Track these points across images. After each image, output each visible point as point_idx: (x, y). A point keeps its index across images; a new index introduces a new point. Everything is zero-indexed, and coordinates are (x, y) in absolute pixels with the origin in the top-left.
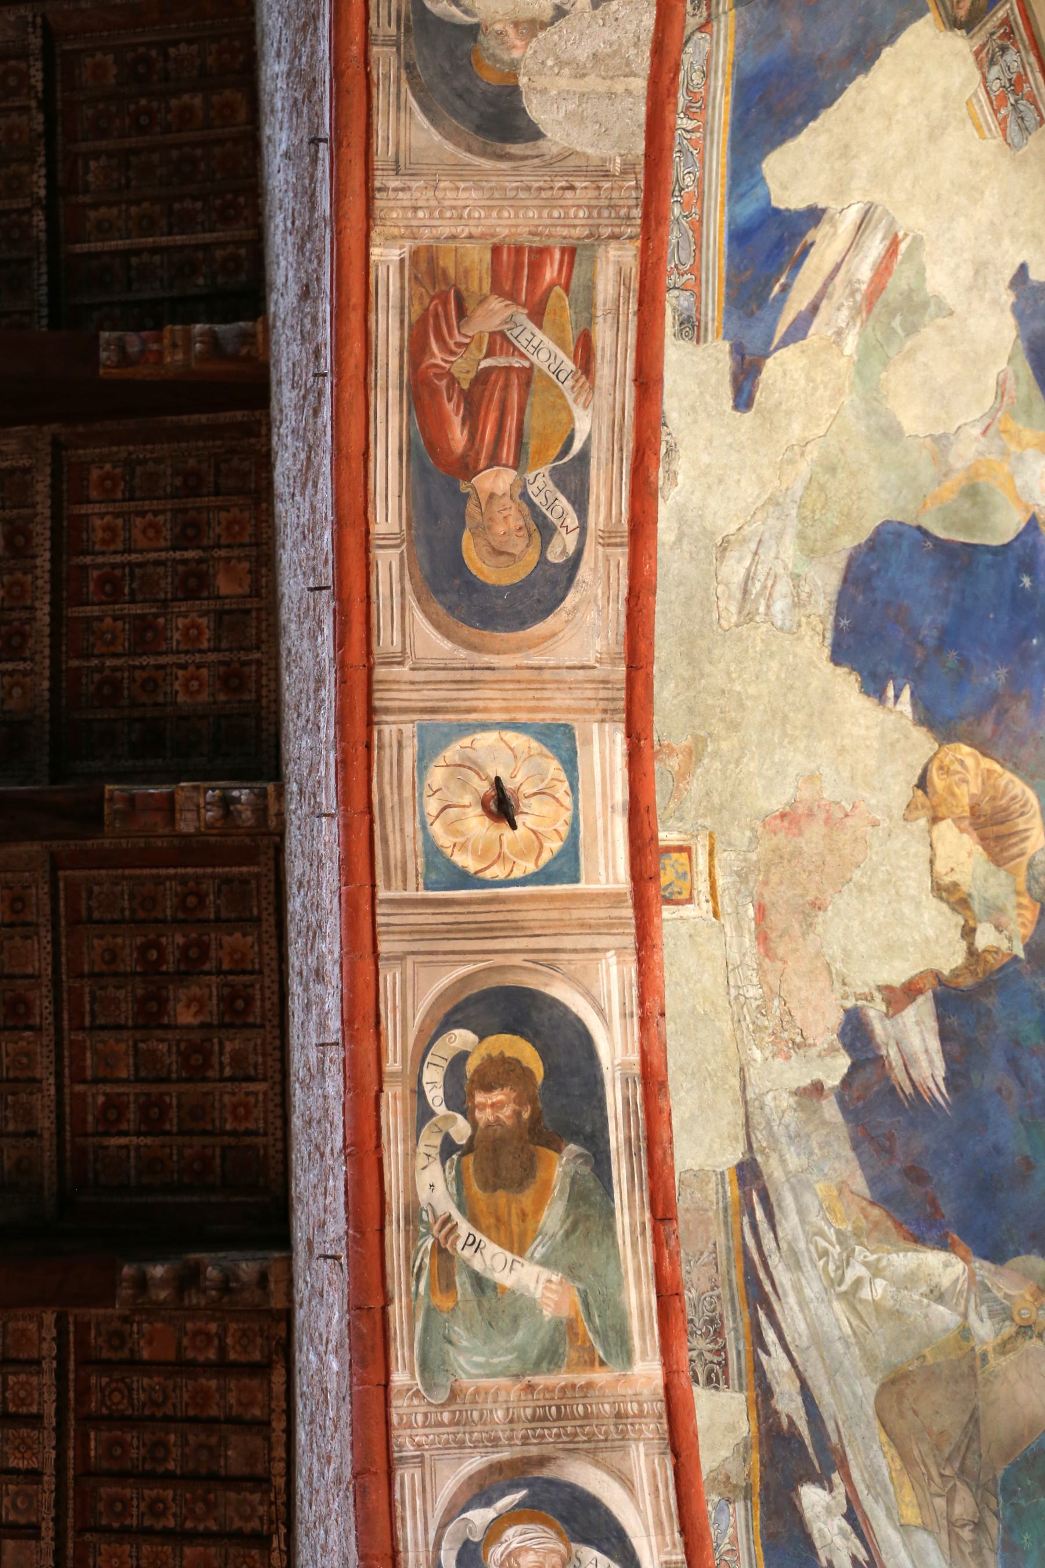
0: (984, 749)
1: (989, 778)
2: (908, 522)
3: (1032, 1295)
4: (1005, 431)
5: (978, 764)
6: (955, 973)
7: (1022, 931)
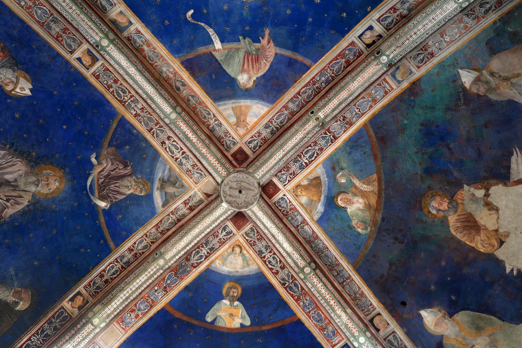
0: (473, 249)
1: (472, 240)
2: (508, 324)
3: (500, 89)
4: (464, 345)
5: (476, 245)
6: (497, 184)
7: (463, 192)
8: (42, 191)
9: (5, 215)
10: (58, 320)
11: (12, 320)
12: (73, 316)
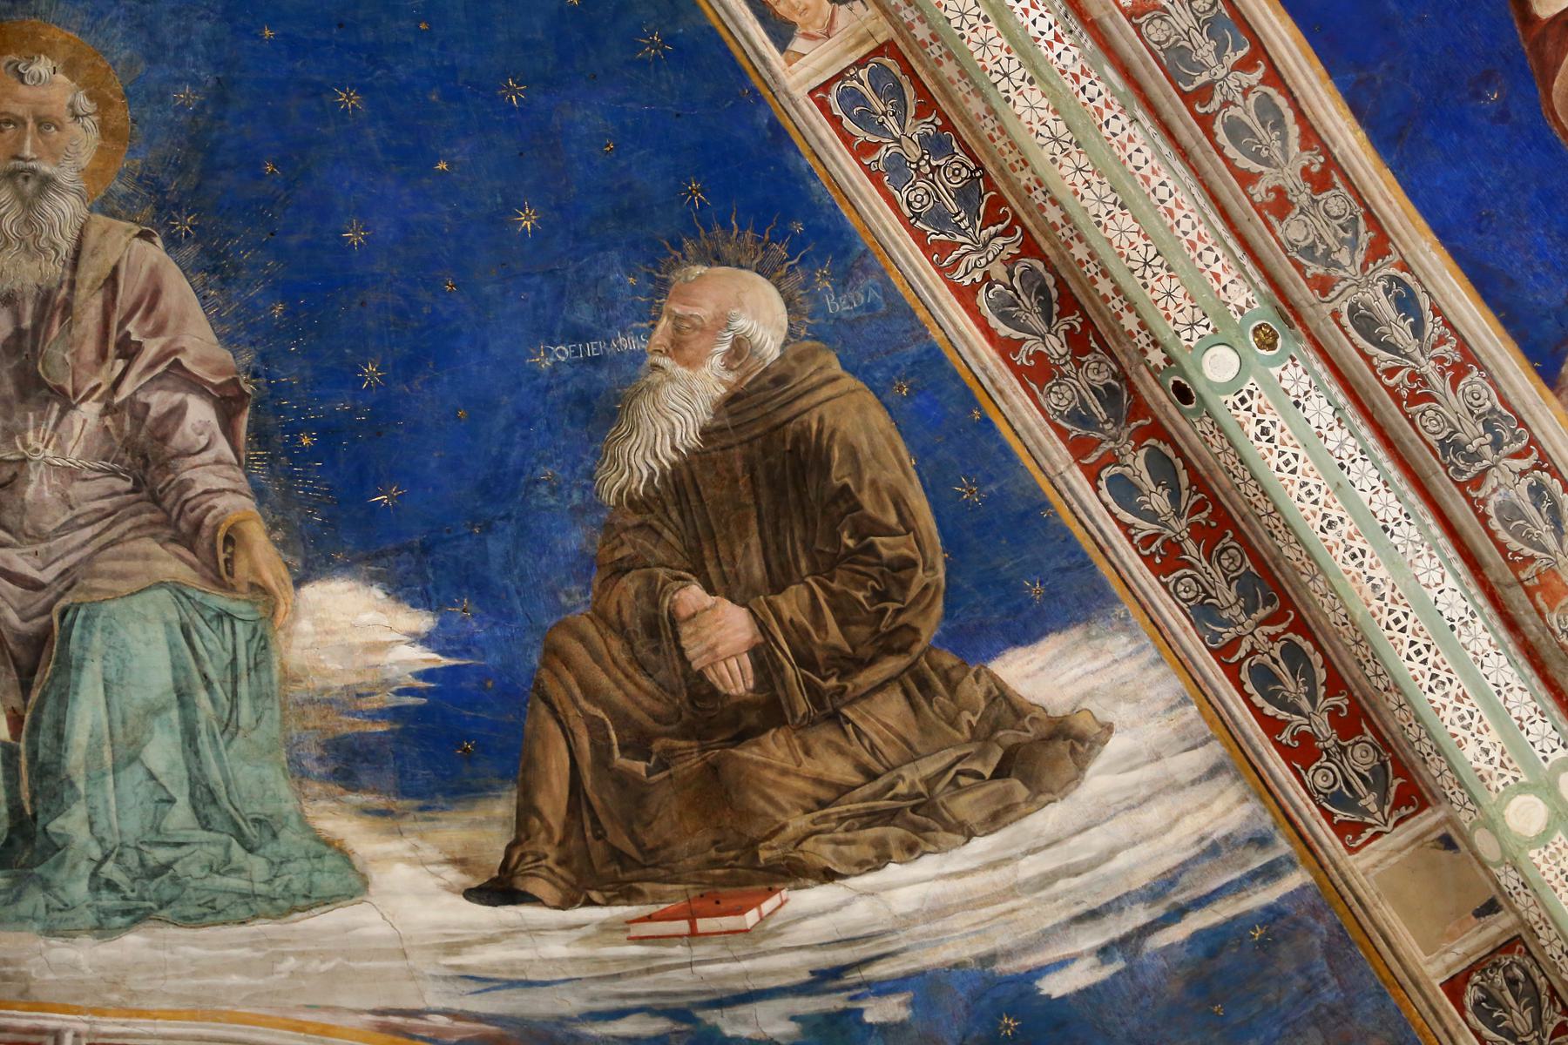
8: (85, 160)
9: (220, 372)
10: (891, 123)
11: (834, 379)
12: (881, 39)
